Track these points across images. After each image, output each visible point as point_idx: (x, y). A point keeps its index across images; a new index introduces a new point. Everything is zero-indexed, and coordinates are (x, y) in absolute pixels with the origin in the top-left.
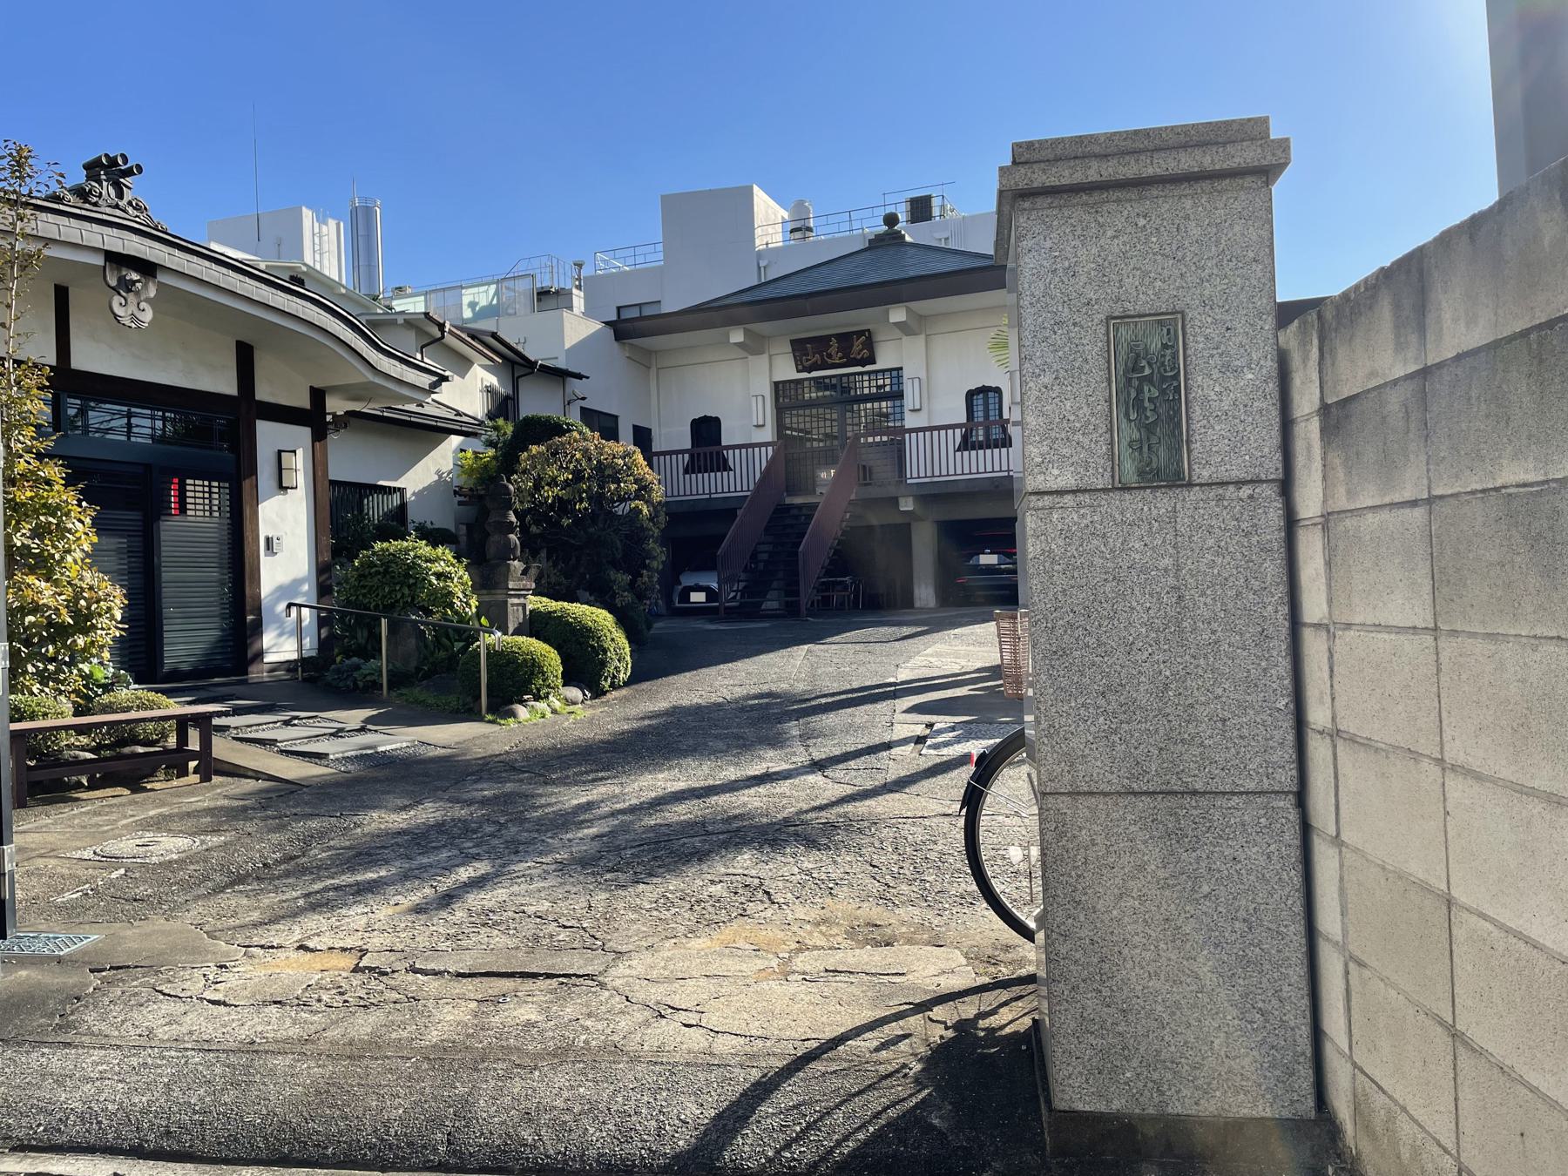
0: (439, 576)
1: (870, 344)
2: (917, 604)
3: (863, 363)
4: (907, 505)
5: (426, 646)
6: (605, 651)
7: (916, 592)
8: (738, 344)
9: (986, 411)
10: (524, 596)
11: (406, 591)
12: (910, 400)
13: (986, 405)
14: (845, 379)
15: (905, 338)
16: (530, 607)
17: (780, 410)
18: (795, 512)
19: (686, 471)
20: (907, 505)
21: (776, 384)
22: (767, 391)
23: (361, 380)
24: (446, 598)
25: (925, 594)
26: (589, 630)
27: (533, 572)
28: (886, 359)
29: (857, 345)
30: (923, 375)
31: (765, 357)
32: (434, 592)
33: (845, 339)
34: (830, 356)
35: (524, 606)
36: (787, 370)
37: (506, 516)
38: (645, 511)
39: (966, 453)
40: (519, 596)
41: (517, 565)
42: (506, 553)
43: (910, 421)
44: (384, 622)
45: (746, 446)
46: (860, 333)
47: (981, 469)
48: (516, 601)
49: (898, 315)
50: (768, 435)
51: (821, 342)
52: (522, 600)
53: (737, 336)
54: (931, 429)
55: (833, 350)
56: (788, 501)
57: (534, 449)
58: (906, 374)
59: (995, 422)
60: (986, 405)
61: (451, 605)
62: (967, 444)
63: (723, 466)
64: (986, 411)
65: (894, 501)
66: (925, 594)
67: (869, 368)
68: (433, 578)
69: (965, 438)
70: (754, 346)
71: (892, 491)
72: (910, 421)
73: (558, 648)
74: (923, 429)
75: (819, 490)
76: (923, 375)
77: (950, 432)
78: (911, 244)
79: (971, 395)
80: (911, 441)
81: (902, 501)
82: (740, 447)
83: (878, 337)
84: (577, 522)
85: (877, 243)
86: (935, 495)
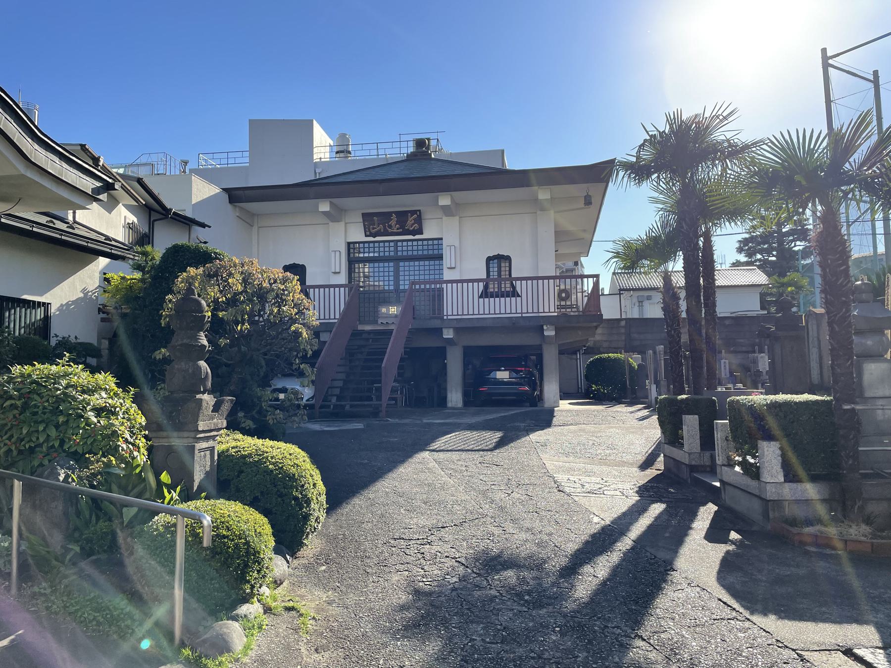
0: (99, 411)
1: (419, 220)
2: (449, 405)
3: (414, 233)
4: (448, 334)
5: (78, 513)
6: (308, 502)
7: (449, 396)
8: (324, 213)
9: (499, 271)
10: (213, 438)
11: (53, 433)
12: (447, 262)
13: (499, 267)
14: (399, 244)
15: (445, 218)
16: (219, 448)
17: (352, 263)
18: (364, 336)
19: (481, 297)
20: (448, 334)
21: (349, 244)
22: (343, 249)
23: (12, 172)
24: (107, 442)
25: (455, 398)
26: (292, 478)
27: (226, 407)
28: (430, 231)
29: (411, 220)
30: (457, 245)
31: (342, 224)
32: (91, 432)
33: (402, 216)
34: (390, 226)
35: (212, 449)
36: (357, 234)
37: (196, 338)
38: (305, 334)
39: (486, 300)
40: (207, 439)
41: (208, 399)
42: (194, 385)
43: (447, 275)
44: (17, 485)
45: (324, 287)
46: (413, 212)
47: (487, 312)
48: (204, 445)
49: (445, 200)
50: (342, 279)
51: (386, 216)
52: (211, 443)
53: (324, 207)
54: (462, 281)
55: (393, 223)
56: (360, 327)
57: (192, 271)
58: (445, 243)
59: (505, 280)
60: (499, 267)
61: (115, 451)
62: (485, 294)
63: (514, 294)
64: (499, 271)
65: (438, 331)
66: (455, 398)
67: (417, 237)
68: (91, 416)
69: (486, 287)
70: (335, 216)
71: (436, 323)
72: (447, 275)
73: (266, 513)
74: (457, 281)
75: (380, 321)
76: (457, 245)
77: (476, 284)
78: (434, 159)
79: (489, 259)
80: (447, 289)
81: (445, 331)
82: (319, 287)
83: (424, 216)
84: (234, 343)
85: (411, 157)
86: (465, 328)
